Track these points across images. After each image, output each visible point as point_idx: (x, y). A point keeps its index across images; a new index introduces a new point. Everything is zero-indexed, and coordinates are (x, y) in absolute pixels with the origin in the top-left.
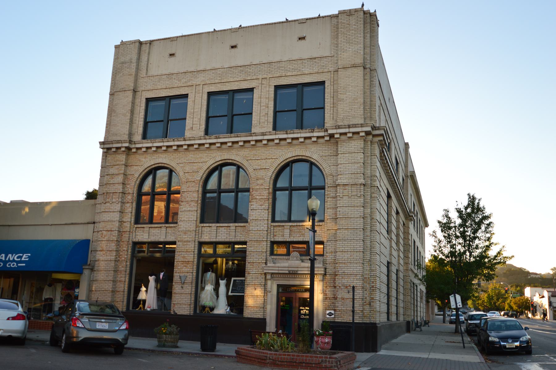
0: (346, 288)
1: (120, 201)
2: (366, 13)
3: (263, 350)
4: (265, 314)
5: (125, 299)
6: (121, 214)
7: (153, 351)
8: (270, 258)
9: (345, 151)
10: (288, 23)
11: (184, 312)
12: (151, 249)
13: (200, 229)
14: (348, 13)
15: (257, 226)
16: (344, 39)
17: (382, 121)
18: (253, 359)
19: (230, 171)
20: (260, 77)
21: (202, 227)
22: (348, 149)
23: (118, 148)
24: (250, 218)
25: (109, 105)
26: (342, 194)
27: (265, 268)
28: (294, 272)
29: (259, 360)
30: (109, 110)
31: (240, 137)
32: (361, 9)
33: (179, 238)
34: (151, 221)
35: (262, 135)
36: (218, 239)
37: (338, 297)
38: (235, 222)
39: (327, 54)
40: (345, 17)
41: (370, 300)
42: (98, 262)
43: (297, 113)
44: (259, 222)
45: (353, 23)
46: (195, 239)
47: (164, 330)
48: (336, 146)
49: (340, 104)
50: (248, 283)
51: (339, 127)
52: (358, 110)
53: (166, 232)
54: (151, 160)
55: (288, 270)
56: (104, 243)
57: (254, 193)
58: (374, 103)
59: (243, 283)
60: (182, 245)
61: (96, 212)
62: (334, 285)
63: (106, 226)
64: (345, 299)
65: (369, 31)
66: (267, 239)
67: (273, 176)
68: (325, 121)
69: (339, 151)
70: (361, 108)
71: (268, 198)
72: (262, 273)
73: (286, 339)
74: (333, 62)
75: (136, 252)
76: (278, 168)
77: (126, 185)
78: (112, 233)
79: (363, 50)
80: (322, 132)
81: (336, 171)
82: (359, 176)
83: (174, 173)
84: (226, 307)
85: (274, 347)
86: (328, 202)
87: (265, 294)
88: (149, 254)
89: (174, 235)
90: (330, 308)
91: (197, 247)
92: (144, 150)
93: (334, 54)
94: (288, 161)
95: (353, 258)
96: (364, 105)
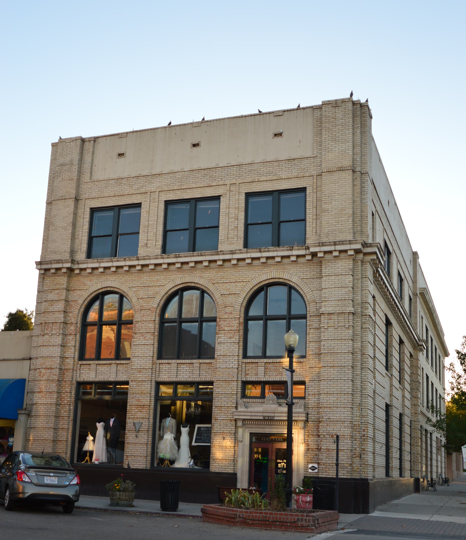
0: (332, 437)
1: (61, 333)
2: (356, 104)
3: (233, 507)
4: (235, 468)
5: (68, 450)
6: (63, 348)
7: (105, 510)
8: (241, 401)
9: (330, 272)
10: (261, 116)
11: (139, 466)
12: (98, 391)
13: (157, 366)
14: (334, 104)
15: (225, 363)
16: (329, 137)
17: (378, 233)
18: (222, 518)
19: (193, 296)
20: (228, 182)
21: (160, 363)
22: (334, 270)
23: (57, 269)
24: (217, 353)
25: (45, 216)
26: (327, 325)
27: (235, 413)
28: (269, 418)
29: (228, 519)
30: (45, 222)
31: (205, 255)
32: (349, 99)
33: (133, 378)
34: (98, 357)
35: (230, 254)
36: (178, 379)
37: (322, 448)
38: (199, 358)
39: (309, 154)
40: (330, 108)
41: (360, 452)
42: (36, 406)
43: (272, 227)
44: (227, 358)
45: (340, 117)
46: (152, 379)
47: (118, 486)
48: (319, 266)
49: (324, 216)
50: (214, 431)
51: (323, 244)
52: (346, 223)
53: (117, 370)
54: (97, 283)
55: (263, 416)
56: (43, 383)
57: (222, 323)
58: (366, 213)
59: (209, 431)
60: (135, 386)
61: (33, 346)
62: (318, 434)
63: (44, 363)
64: (330, 450)
65: (359, 126)
66: (238, 378)
67: (245, 303)
68: (307, 237)
69: (323, 273)
70: (350, 220)
71: (238, 329)
72: (231, 419)
73: (258, 496)
74: (316, 164)
75: (81, 394)
76: (251, 293)
77: (68, 313)
78: (52, 371)
79: (351, 149)
80: (303, 249)
81: (320, 297)
82: (348, 303)
83: (125, 299)
84: (190, 460)
85: (244, 505)
86: (310, 334)
87: (235, 444)
88: (97, 396)
89: (126, 373)
90: (312, 461)
91: (154, 388)
92: (89, 271)
93: (317, 154)
94: (262, 284)
95: (339, 401)
96: (353, 217)
